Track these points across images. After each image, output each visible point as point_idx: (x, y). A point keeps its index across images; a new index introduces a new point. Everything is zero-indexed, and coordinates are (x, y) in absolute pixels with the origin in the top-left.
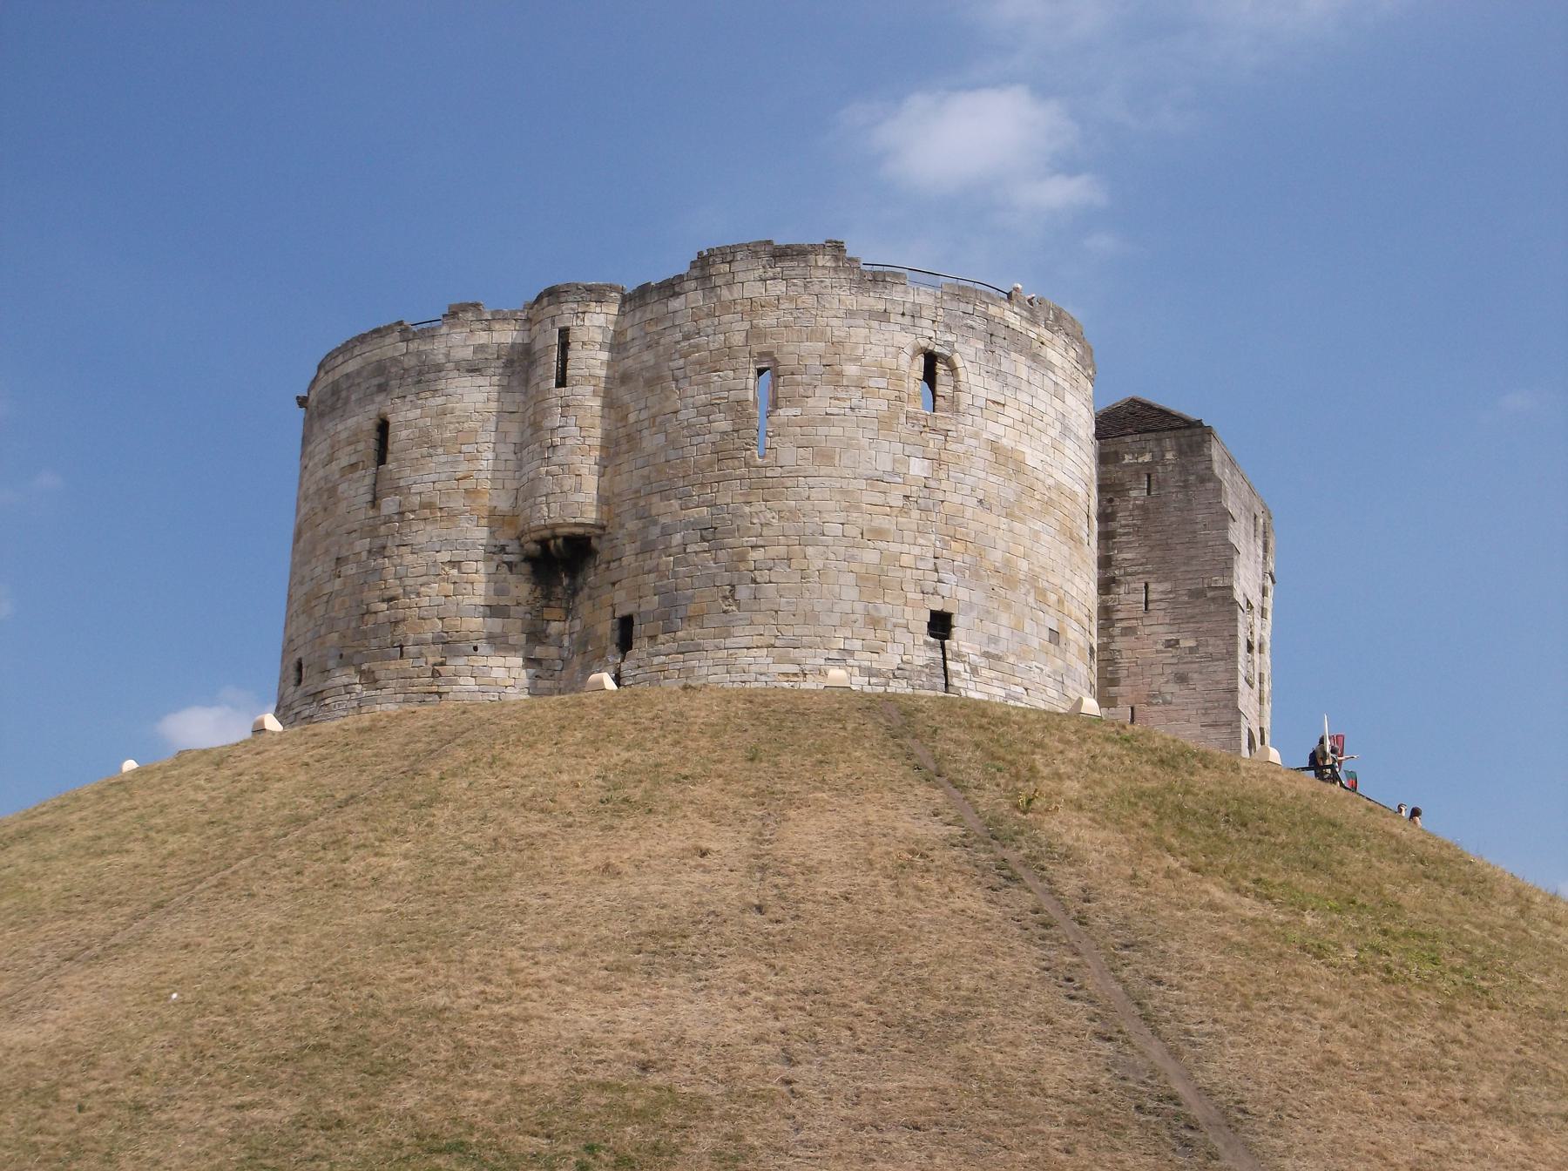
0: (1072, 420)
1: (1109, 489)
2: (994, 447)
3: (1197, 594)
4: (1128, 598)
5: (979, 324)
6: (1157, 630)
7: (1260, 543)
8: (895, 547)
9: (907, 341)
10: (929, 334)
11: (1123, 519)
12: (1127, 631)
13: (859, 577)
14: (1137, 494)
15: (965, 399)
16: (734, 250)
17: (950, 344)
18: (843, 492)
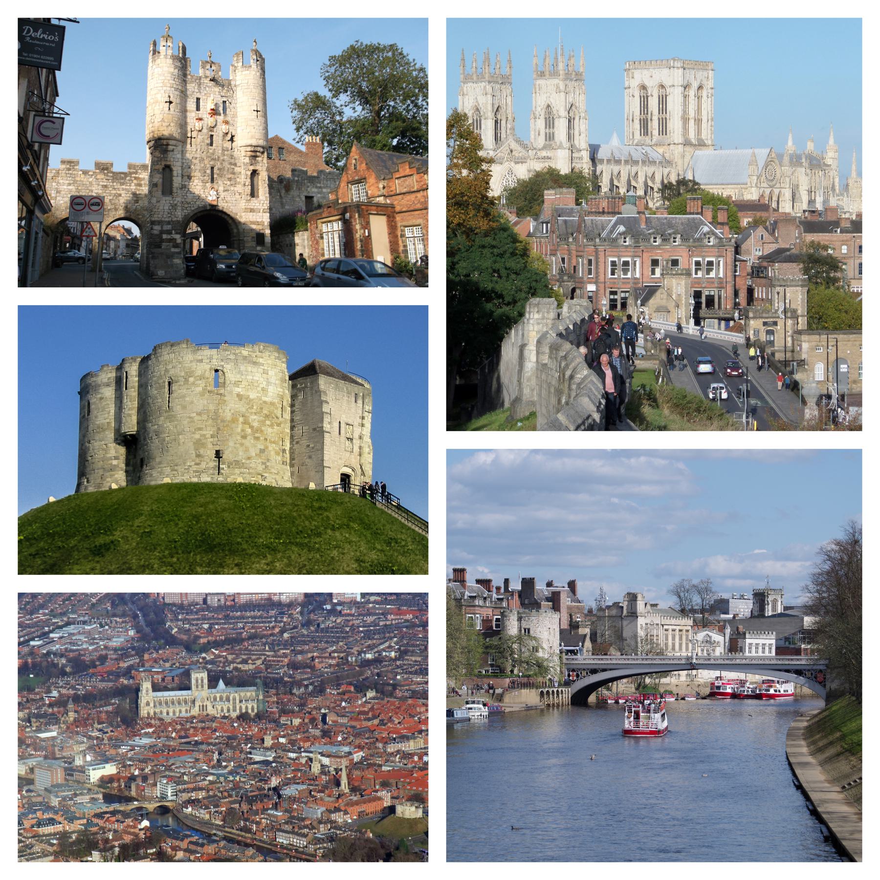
0: (273, 380)
1: (293, 397)
2: (238, 395)
3: (314, 429)
4: (298, 431)
5: (232, 357)
6: (304, 442)
7: (360, 402)
8: (204, 433)
9: (208, 367)
10: (216, 363)
11: (297, 406)
12: (297, 443)
13: (194, 443)
14: (301, 397)
15: (228, 382)
16: (162, 345)
17: (223, 366)
18: (190, 417)
